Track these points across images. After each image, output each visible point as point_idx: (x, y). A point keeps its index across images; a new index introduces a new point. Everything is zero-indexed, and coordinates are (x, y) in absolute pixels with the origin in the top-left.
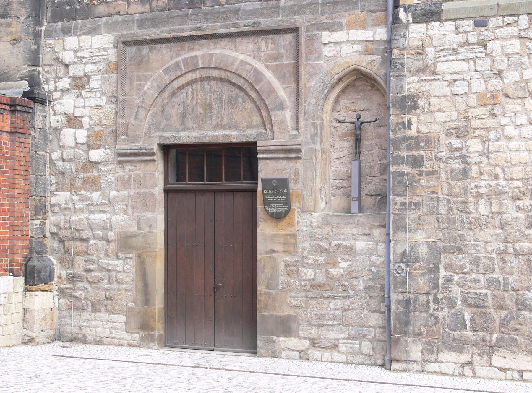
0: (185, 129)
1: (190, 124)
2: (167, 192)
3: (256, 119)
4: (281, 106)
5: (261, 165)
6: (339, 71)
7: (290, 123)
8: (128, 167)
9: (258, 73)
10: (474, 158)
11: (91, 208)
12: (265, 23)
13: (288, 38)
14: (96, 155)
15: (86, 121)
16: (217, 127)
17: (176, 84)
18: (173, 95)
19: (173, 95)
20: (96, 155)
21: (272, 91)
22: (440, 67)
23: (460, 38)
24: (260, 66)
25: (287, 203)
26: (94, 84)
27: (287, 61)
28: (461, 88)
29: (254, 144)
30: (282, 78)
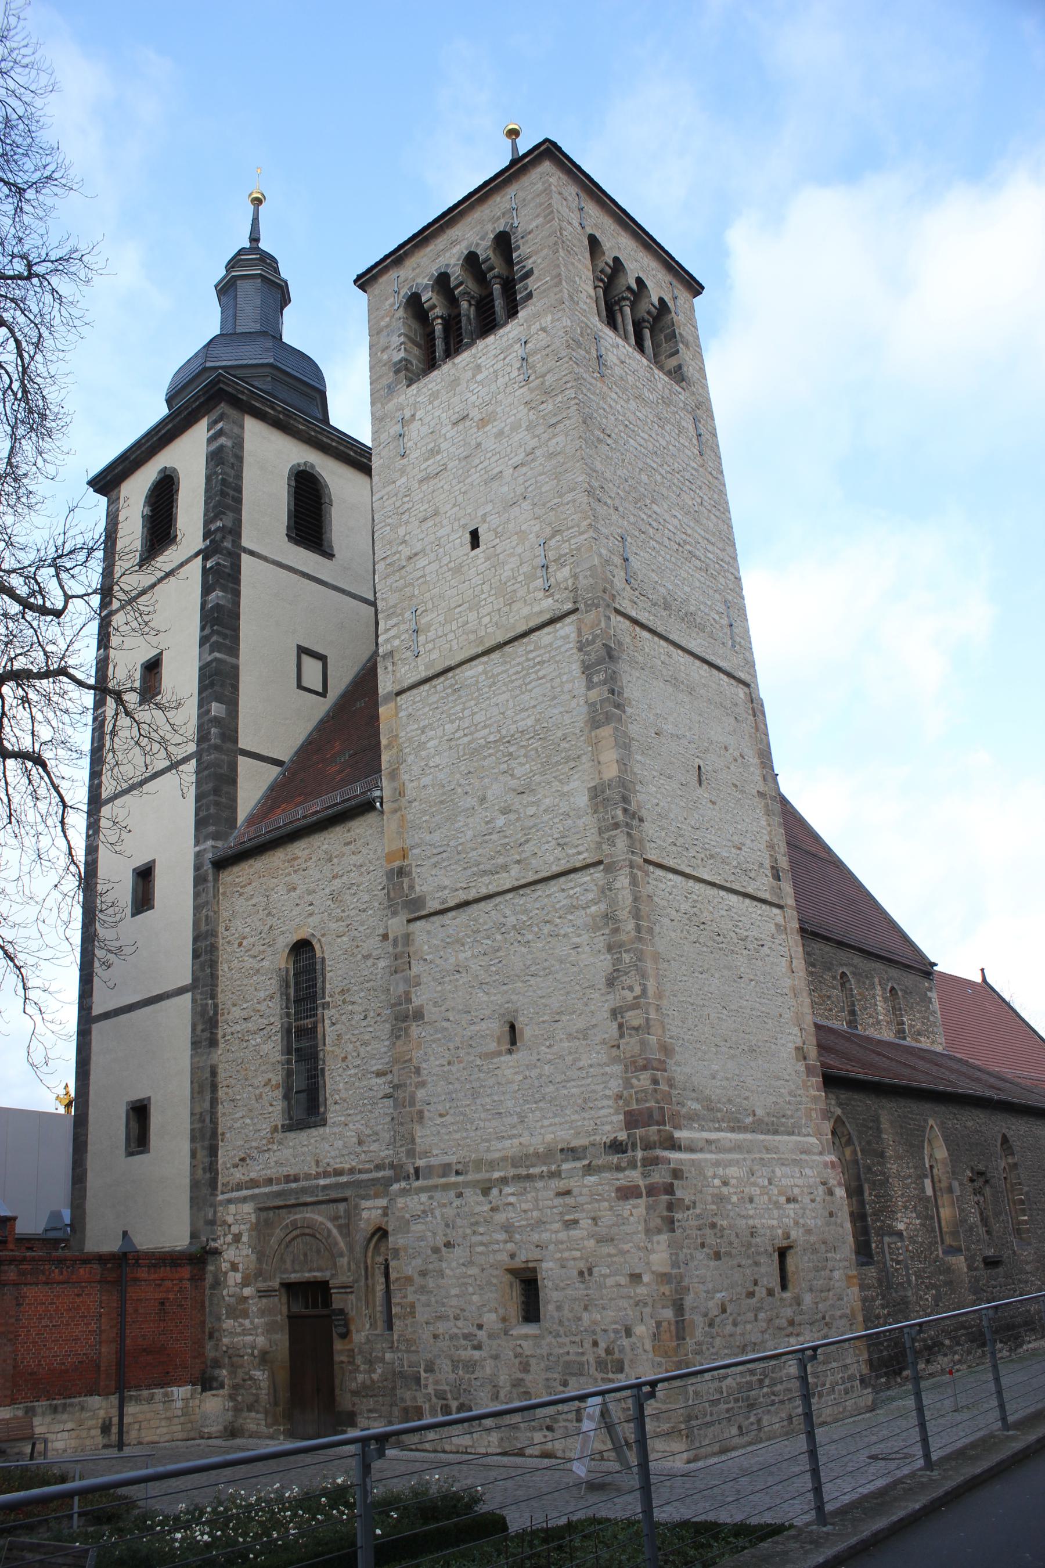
0: (295, 1271)
4: (342, 1255)
6: (371, 1229)
7: (346, 1267)
8: (264, 1300)
9: (329, 1231)
11: (245, 1332)
13: (342, 1207)
14: (247, 1291)
15: (241, 1266)
16: (310, 1271)
17: (288, 1239)
18: (287, 1246)
19: (287, 1246)
20: (247, 1291)
21: (336, 1244)
25: (346, 1325)
26: (245, 1238)
29: (327, 1282)
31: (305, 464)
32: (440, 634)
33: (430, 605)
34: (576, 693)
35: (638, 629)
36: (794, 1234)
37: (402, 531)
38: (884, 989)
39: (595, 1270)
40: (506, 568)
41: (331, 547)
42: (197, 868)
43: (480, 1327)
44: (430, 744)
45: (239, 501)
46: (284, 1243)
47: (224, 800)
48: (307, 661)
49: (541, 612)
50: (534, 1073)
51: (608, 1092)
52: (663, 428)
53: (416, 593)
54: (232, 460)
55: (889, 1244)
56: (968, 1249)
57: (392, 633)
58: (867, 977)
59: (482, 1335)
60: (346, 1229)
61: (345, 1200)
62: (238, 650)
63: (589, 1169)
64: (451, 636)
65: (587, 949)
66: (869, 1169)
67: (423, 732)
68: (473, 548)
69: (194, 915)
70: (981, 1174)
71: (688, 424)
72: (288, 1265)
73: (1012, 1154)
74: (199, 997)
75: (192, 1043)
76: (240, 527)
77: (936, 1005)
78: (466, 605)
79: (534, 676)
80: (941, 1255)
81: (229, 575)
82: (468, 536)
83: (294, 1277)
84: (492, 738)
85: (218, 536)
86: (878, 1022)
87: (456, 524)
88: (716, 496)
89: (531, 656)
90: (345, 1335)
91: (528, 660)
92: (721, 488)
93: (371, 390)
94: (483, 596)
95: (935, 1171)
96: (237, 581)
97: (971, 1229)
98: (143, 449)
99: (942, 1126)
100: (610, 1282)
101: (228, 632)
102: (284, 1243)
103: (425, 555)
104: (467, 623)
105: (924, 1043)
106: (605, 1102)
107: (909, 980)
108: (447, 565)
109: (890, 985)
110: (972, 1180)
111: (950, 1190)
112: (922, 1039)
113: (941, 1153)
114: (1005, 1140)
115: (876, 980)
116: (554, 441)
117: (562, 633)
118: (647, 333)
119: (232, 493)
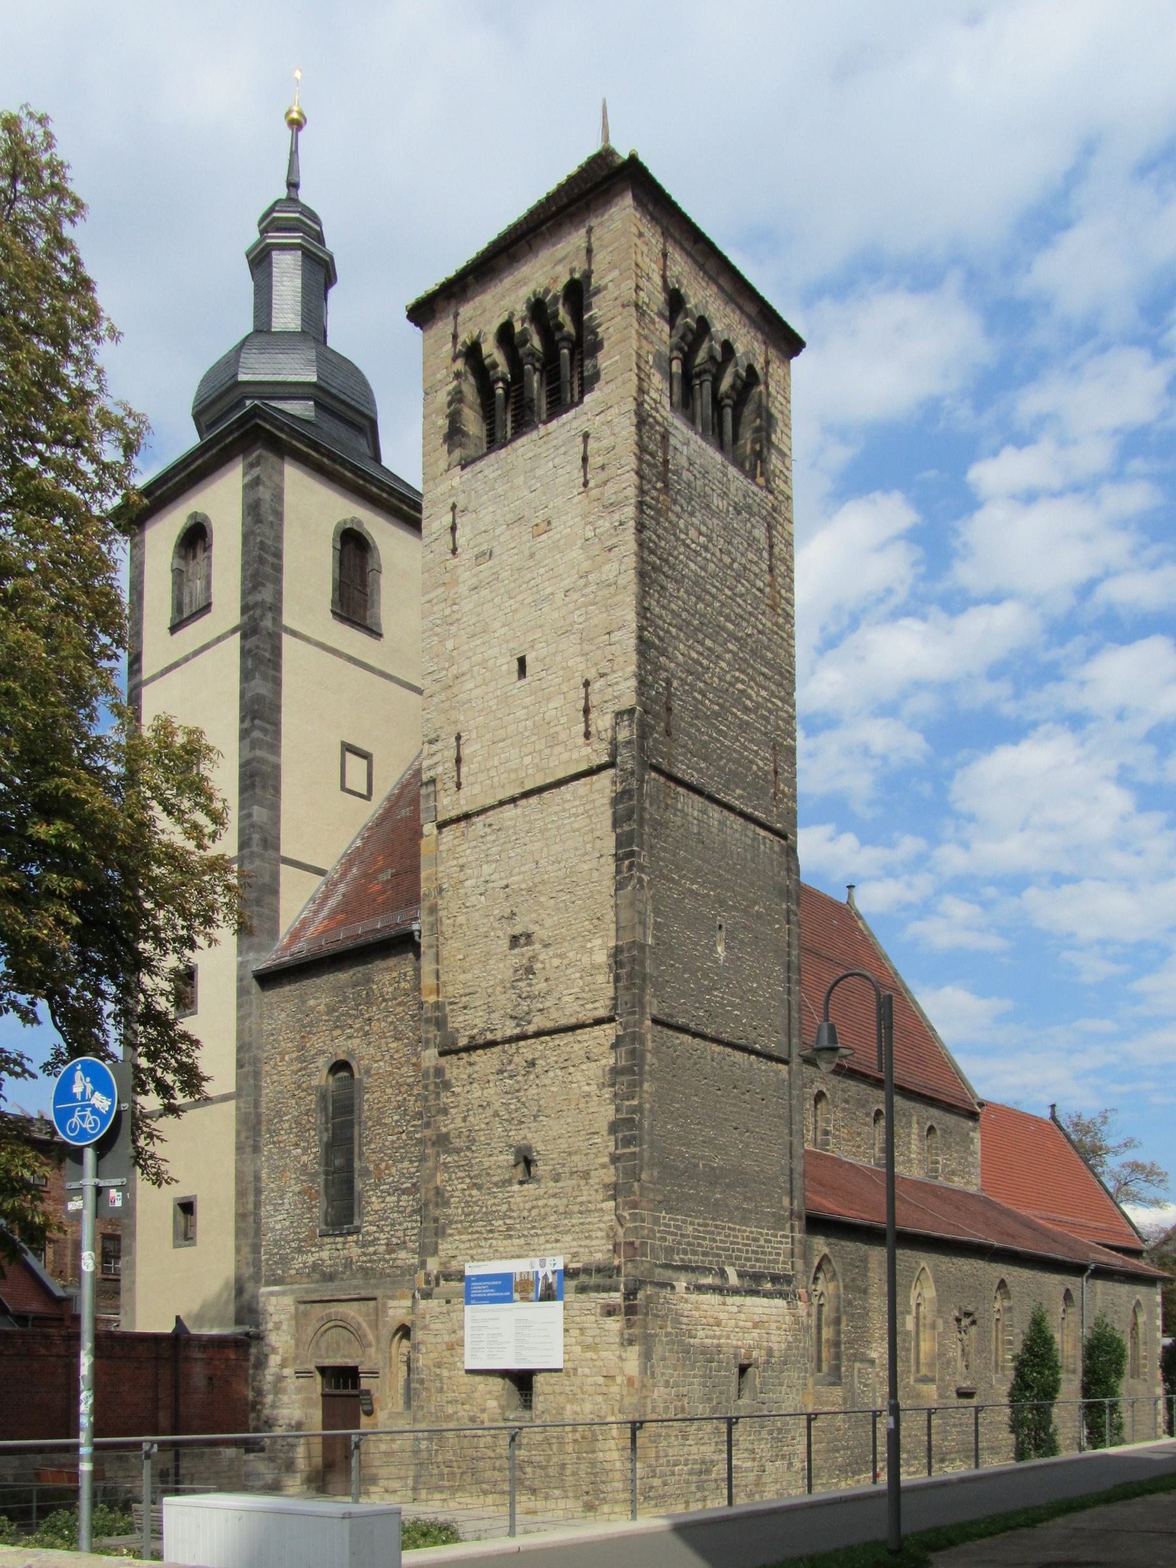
1: (330, 1354)
2: (323, 1395)
3: (360, 1352)
4: (370, 1345)
5: (362, 1380)
6: (395, 1326)
9: (359, 1324)
10: (445, 1380)
12: (364, 1294)
13: (372, 1303)
17: (323, 1329)
18: (322, 1335)
21: (365, 1336)
22: (432, 1326)
23: (439, 1310)
24: (360, 1319)
27: (373, 1317)
28: (439, 1340)
29: (356, 1368)
30: (371, 1327)
31: (353, 520)
32: (483, 767)
33: (474, 735)
34: (605, 851)
35: (672, 785)
36: (755, 1354)
37: (450, 645)
38: (921, 1128)
39: (580, 1370)
40: (552, 705)
41: (379, 625)
42: (240, 979)
43: (483, 1411)
44: (468, 883)
45: (278, 569)
46: (319, 1333)
47: (266, 911)
48: (352, 759)
49: (578, 761)
50: (541, 1203)
51: (602, 1225)
52: (730, 543)
53: (462, 718)
54: (271, 518)
55: (859, 1370)
56: (942, 1380)
57: (436, 759)
58: (904, 1115)
59: (485, 1416)
60: (375, 1325)
61: (374, 1299)
62: (279, 747)
63: (582, 1289)
64: (493, 773)
65: (595, 1098)
66: (850, 1303)
67: (461, 871)
68: (520, 679)
69: (238, 1025)
70: (968, 1314)
71: (760, 533)
72: (323, 1352)
73: (1009, 1298)
74: (242, 1105)
75: (237, 1149)
76: (280, 601)
77: (977, 1145)
78: (509, 741)
79: (568, 827)
80: (912, 1382)
81: (270, 660)
82: (516, 665)
83: (328, 1362)
84: (523, 886)
85: (258, 612)
86: (910, 1161)
87: (505, 646)
88: (781, 620)
89: (567, 806)
90: (369, 1413)
91: (564, 810)
92: (788, 608)
93: (424, 463)
94: (526, 734)
95: (922, 1308)
96: (277, 666)
97: (949, 1362)
98: (170, 484)
99: (935, 1268)
100: (590, 1380)
101: (268, 726)
102: (319, 1333)
103: (472, 677)
104: (509, 760)
105: (958, 1183)
106: (599, 1234)
107: (951, 1120)
108: (493, 692)
109: (929, 1124)
110: (958, 1320)
111: (933, 1326)
112: (956, 1179)
113: (930, 1292)
114: (1002, 1284)
115: (914, 1119)
116: (608, 567)
117: (597, 786)
118: (728, 412)
119: (270, 559)
